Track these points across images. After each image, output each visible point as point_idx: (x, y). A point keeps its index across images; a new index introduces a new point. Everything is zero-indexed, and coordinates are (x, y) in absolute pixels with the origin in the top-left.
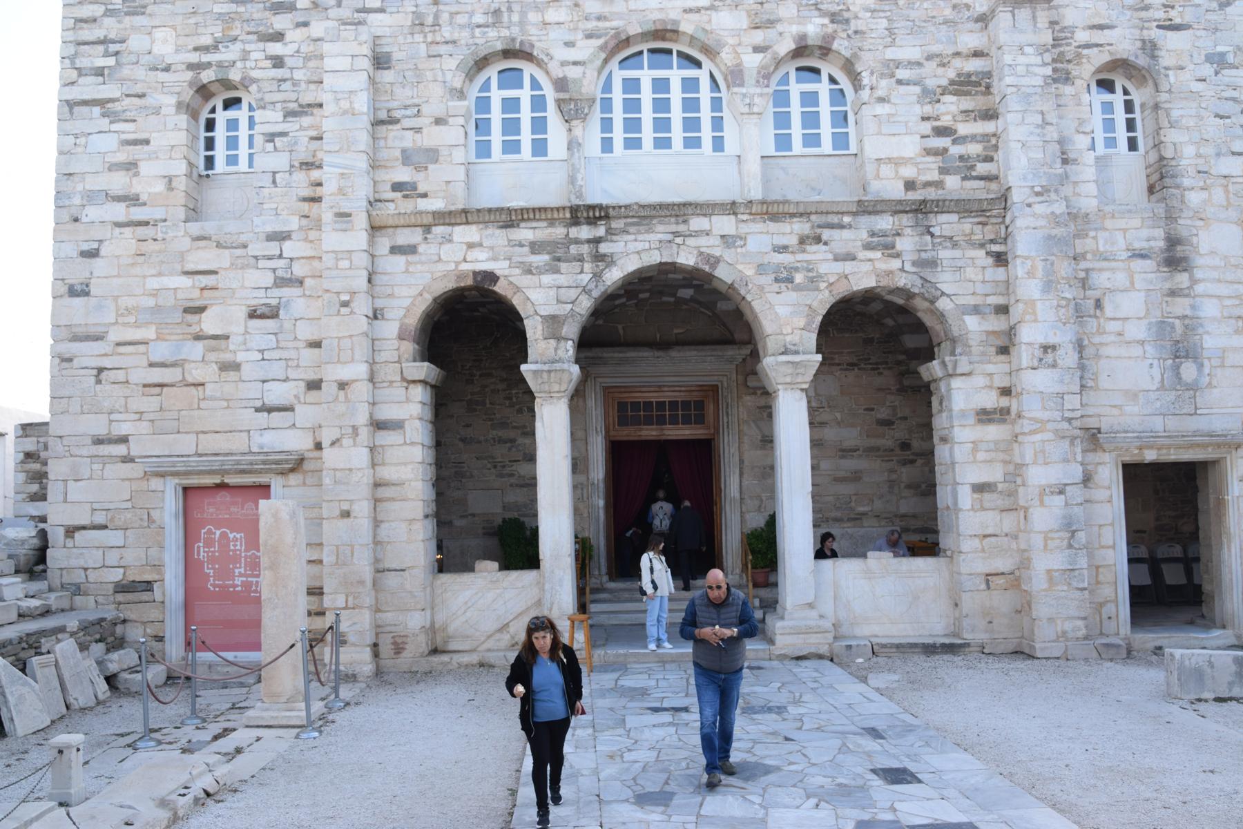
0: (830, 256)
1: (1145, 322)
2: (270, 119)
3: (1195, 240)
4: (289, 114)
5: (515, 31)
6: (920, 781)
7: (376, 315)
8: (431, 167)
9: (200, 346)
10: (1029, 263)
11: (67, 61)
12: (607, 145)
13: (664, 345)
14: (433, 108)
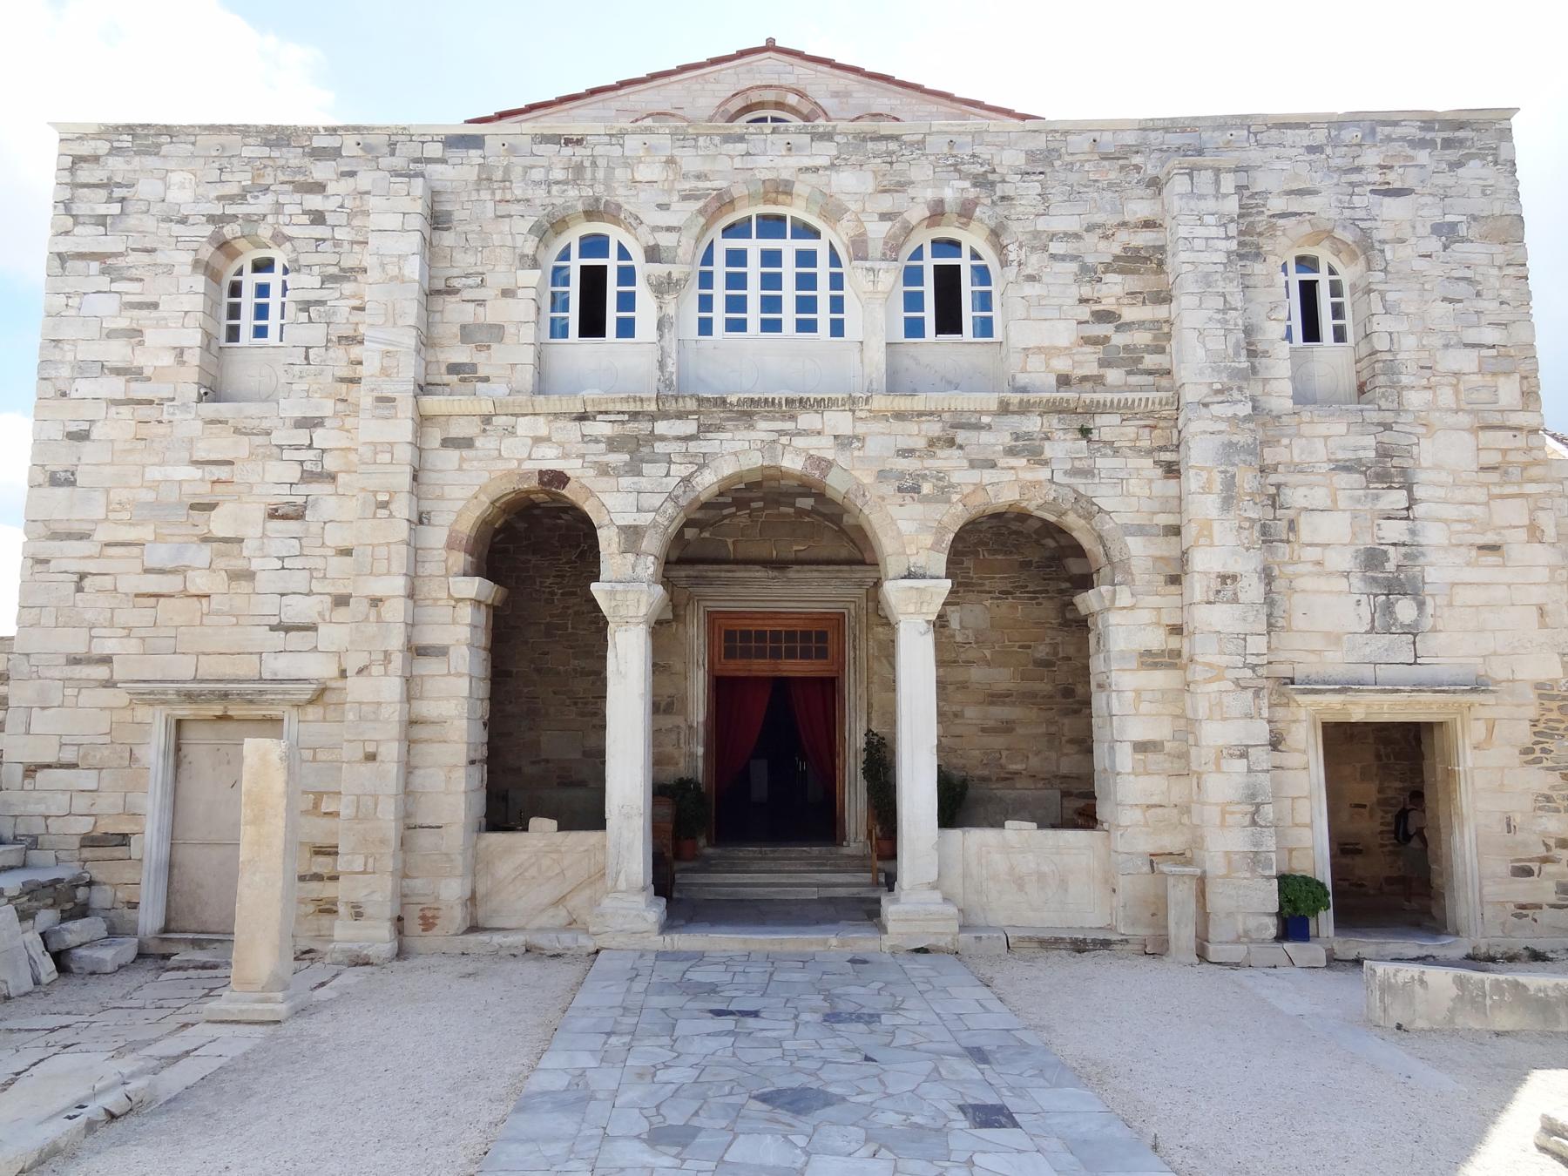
0: (966, 464)
1: (1353, 548)
2: (306, 284)
3: (1415, 450)
4: (326, 279)
5: (600, 189)
6: (1016, 1125)
7: (421, 519)
8: (494, 346)
9: (206, 551)
10: (1205, 475)
11: (61, 206)
12: (705, 327)
13: (780, 565)
14: (499, 277)
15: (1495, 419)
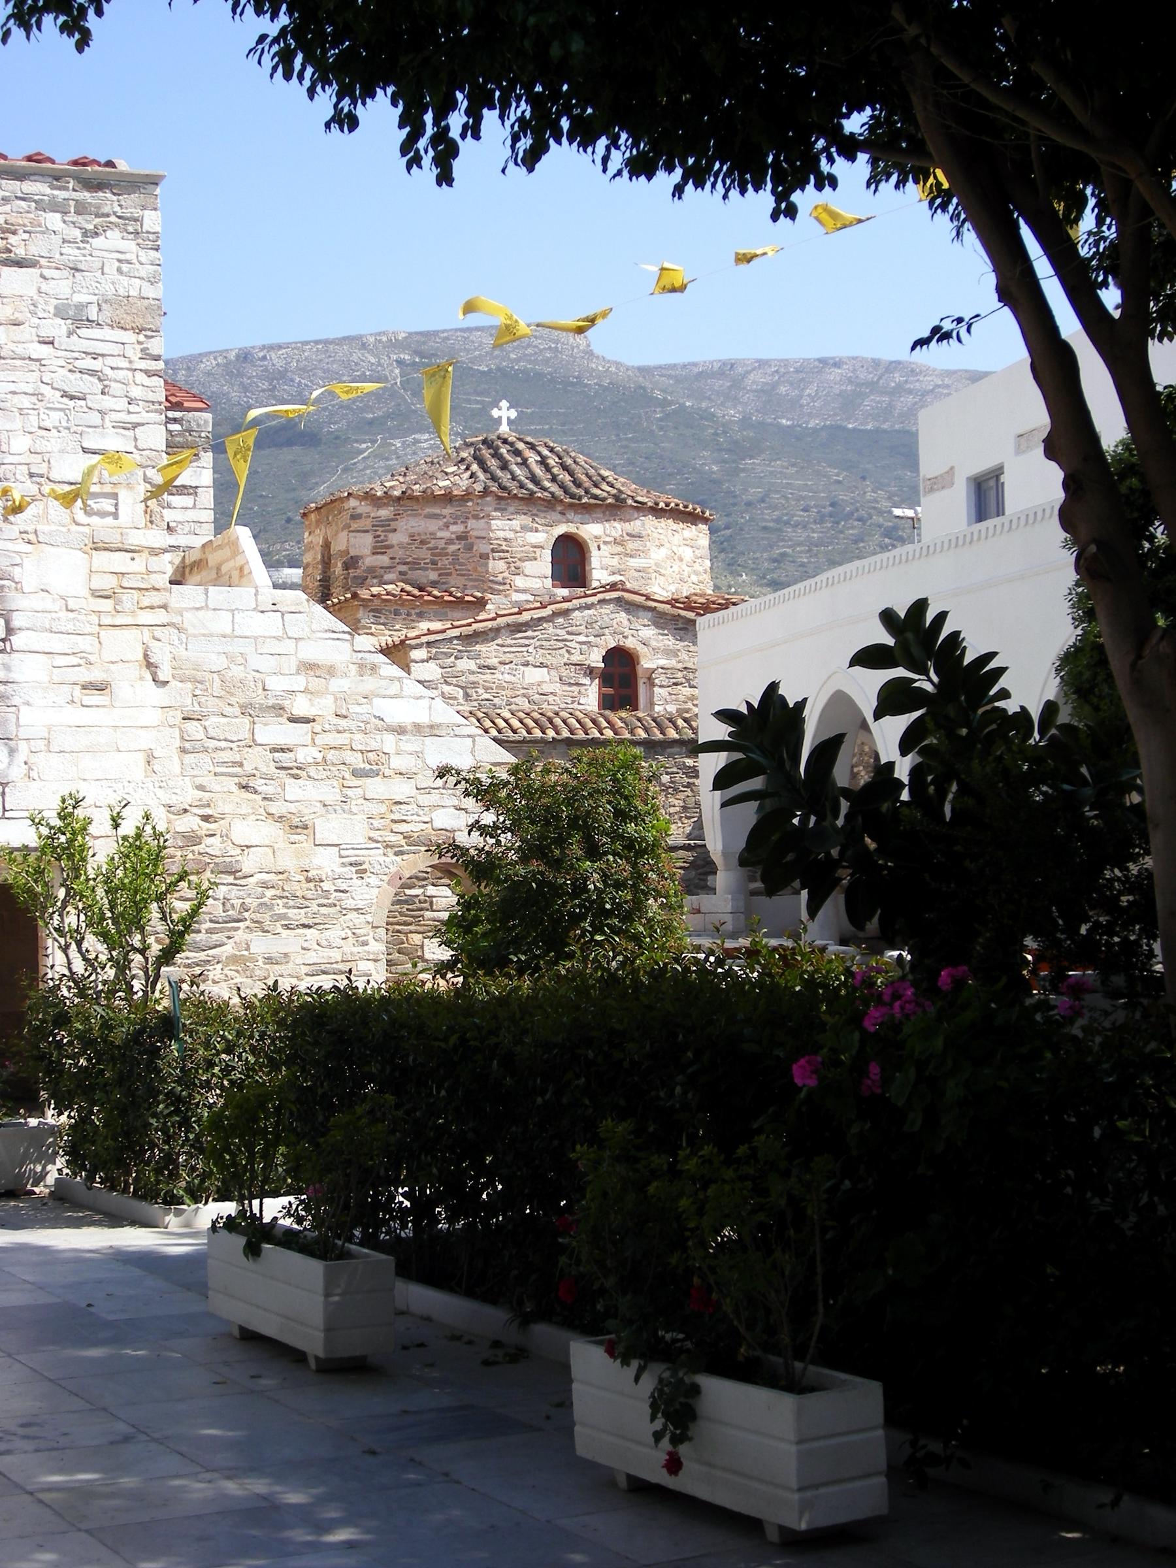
15: (114, 539)
